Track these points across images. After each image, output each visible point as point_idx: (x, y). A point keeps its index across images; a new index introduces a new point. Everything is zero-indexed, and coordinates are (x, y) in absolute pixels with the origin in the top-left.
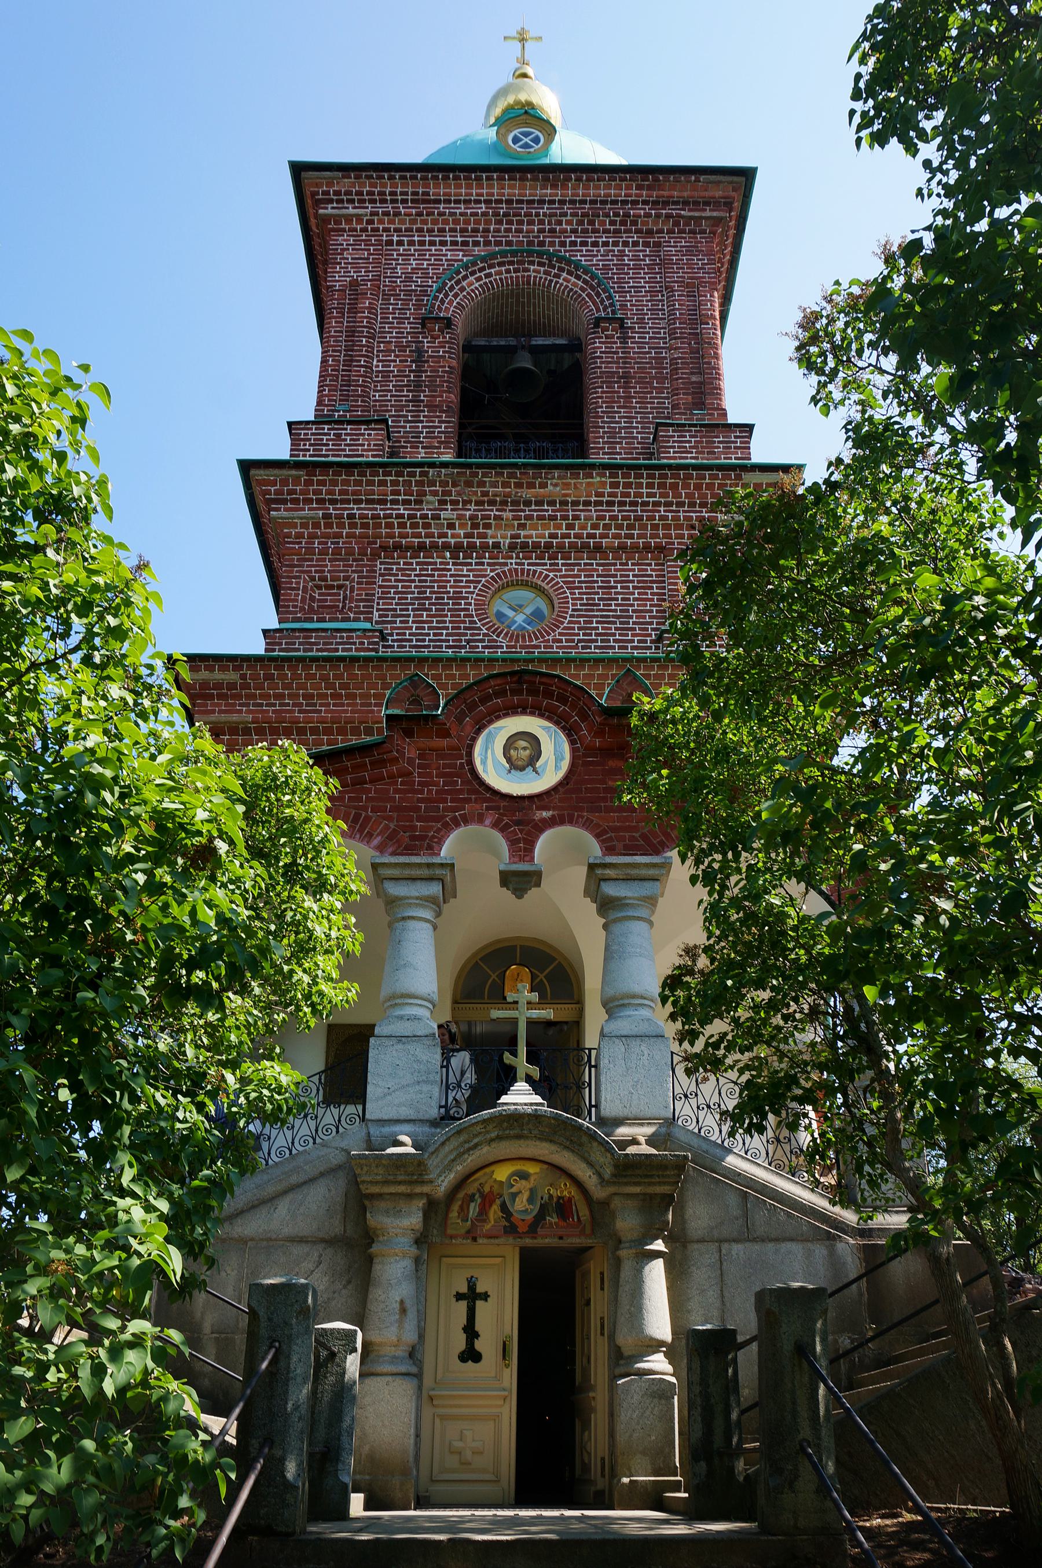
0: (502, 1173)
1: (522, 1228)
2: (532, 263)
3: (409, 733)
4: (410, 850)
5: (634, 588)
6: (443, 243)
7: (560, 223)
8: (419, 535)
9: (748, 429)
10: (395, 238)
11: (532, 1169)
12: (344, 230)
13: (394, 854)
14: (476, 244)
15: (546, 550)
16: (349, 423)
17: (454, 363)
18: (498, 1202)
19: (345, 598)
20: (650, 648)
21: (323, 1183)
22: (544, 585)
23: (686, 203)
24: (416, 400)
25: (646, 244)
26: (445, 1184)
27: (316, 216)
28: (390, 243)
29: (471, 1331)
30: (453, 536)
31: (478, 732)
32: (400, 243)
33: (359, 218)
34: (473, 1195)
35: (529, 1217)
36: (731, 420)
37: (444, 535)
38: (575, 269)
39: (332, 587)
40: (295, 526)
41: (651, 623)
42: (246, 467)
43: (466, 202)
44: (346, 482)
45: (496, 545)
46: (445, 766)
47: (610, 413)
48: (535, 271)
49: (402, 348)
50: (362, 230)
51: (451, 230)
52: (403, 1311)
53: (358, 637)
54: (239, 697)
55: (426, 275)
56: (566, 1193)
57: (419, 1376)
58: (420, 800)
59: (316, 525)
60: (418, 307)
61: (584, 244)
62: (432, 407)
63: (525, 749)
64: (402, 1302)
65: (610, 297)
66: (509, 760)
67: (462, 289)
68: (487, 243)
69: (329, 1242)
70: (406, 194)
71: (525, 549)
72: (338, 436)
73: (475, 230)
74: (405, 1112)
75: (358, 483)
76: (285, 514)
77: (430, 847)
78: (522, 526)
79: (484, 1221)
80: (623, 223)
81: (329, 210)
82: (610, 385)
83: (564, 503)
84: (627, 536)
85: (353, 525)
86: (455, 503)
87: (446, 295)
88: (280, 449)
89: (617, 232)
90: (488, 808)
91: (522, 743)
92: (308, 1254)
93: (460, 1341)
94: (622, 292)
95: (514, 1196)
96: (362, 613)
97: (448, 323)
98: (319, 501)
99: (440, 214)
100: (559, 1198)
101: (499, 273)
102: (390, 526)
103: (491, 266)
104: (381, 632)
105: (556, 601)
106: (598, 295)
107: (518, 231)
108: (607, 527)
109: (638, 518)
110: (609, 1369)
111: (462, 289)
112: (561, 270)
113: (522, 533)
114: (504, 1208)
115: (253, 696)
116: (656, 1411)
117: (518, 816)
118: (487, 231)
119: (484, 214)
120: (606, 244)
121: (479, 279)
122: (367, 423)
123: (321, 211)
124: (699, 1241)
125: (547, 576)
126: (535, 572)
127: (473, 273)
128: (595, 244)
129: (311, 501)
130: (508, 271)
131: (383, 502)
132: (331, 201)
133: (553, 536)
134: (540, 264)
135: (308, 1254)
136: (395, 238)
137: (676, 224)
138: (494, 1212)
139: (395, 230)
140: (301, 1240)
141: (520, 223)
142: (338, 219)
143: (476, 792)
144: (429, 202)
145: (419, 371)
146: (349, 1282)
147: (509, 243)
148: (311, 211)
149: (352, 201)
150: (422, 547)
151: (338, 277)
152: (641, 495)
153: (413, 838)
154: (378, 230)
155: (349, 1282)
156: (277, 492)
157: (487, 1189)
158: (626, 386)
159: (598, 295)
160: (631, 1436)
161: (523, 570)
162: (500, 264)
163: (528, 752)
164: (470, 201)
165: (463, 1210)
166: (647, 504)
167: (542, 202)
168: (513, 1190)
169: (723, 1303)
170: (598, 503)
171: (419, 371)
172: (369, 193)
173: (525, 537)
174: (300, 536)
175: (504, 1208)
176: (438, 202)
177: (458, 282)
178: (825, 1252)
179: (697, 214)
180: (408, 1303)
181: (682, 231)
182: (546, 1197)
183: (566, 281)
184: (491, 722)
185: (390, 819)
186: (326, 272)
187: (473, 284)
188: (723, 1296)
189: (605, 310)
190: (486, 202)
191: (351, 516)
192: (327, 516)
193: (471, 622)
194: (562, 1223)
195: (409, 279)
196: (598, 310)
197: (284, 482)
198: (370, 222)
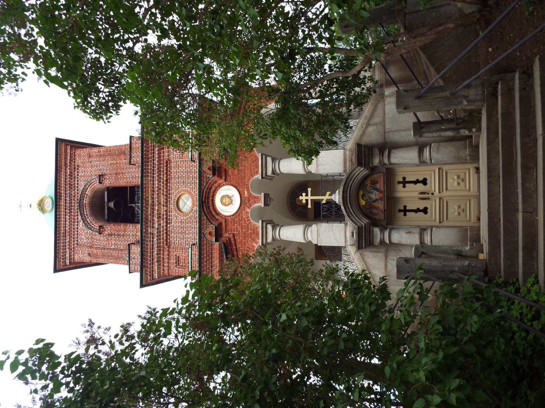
0: (363, 203)
1: (381, 195)
2: (83, 202)
3: (221, 235)
4: (257, 234)
5: (178, 169)
6: (77, 228)
7: (72, 194)
9: (131, 137)
10: (76, 242)
11: (361, 193)
12: (74, 257)
13: (259, 239)
14: (78, 218)
15: (167, 197)
16: (129, 255)
17: (112, 225)
18: (372, 203)
19: (182, 256)
20: (197, 164)
21: (366, 259)
22: (178, 197)
24: (123, 235)
25: (78, 169)
26: (366, 220)
27: (69, 265)
28: (77, 244)
29: (417, 211)
30: (163, 224)
31: (220, 214)
32: (77, 241)
33: (70, 253)
34: (370, 211)
35: (377, 193)
36: (128, 143)
37: (163, 226)
38: (85, 190)
39: (178, 260)
41: (189, 164)
42: (142, 285)
43: (65, 222)
45: (166, 211)
46: (231, 224)
47: (127, 178)
48: (86, 201)
49: (108, 240)
50: (74, 252)
52: (410, 232)
53: (194, 252)
55: (87, 233)
56: (369, 182)
57: (432, 227)
58: (242, 231)
59: (160, 265)
60: (96, 235)
61: (78, 187)
62: (125, 231)
63: (226, 200)
64: (406, 233)
65: (93, 179)
66: (229, 204)
67: (91, 222)
68: (77, 215)
69: (386, 257)
70: (63, 239)
72: (133, 258)
74: (343, 234)
77: (257, 228)
78: (160, 203)
79: (379, 208)
80: (72, 176)
81: (68, 262)
82: (118, 178)
84: (163, 172)
85: (160, 254)
87: (93, 227)
88: (137, 276)
90: (244, 210)
91: (224, 200)
92: (391, 264)
93: (422, 214)
94: (92, 176)
95: (370, 198)
96: (186, 251)
97: (101, 227)
98: (153, 264)
99: (69, 229)
100: (371, 184)
102: (160, 243)
103: (84, 214)
104: (192, 245)
105: (183, 193)
106: (92, 183)
108: (160, 178)
109: (158, 169)
110: (429, 166)
111: (91, 222)
113: (162, 203)
114: (375, 201)
116: (444, 149)
117: (247, 201)
119: (69, 216)
120: (78, 181)
121: (88, 218)
122: (129, 250)
123: (68, 264)
124: (385, 139)
125: (175, 196)
126: (174, 199)
127: (86, 219)
128: (78, 184)
130: (86, 209)
131: (153, 244)
132: (65, 261)
135: (391, 264)
136: (76, 242)
138: (376, 204)
139: (74, 242)
140: (386, 266)
141: (72, 206)
142: (70, 259)
143: (239, 214)
144: (65, 232)
145: (114, 235)
146: (400, 250)
147: (77, 209)
148: (68, 267)
149: (65, 255)
150: (167, 233)
151: (87, 259)
153: (254, 233)
154: (74, 247)
155: (400, 250)
157: (368, 207)
158: (119, 174)
159: (92, 183)
160: (453, 157)
161: (173, 203)
162: (84, 212)
163: (227, 199)
164: (65, 221)
165: (375, 214)
166: (153, 166)
168: (368, 199)
169: (406, 130)
171: (114, 235)
173: (163, 202)
175: (375, 201)
176: (65, 230)
177: (89, 224)
178: (388, 98)
179: (69, 155)
180: (407, 231)
181: (74, 158)
182: (371, 188)
183: (89, 192)
184: (217, 210)
185: (248, 240)
186: (86, 263)
187: (89, 219)
188: (404, 130)
189: (96, 180)
190: (65, 216)
193: (189, 218)
194: (379, 183)
196: (97, 183)
198: (71, 250)
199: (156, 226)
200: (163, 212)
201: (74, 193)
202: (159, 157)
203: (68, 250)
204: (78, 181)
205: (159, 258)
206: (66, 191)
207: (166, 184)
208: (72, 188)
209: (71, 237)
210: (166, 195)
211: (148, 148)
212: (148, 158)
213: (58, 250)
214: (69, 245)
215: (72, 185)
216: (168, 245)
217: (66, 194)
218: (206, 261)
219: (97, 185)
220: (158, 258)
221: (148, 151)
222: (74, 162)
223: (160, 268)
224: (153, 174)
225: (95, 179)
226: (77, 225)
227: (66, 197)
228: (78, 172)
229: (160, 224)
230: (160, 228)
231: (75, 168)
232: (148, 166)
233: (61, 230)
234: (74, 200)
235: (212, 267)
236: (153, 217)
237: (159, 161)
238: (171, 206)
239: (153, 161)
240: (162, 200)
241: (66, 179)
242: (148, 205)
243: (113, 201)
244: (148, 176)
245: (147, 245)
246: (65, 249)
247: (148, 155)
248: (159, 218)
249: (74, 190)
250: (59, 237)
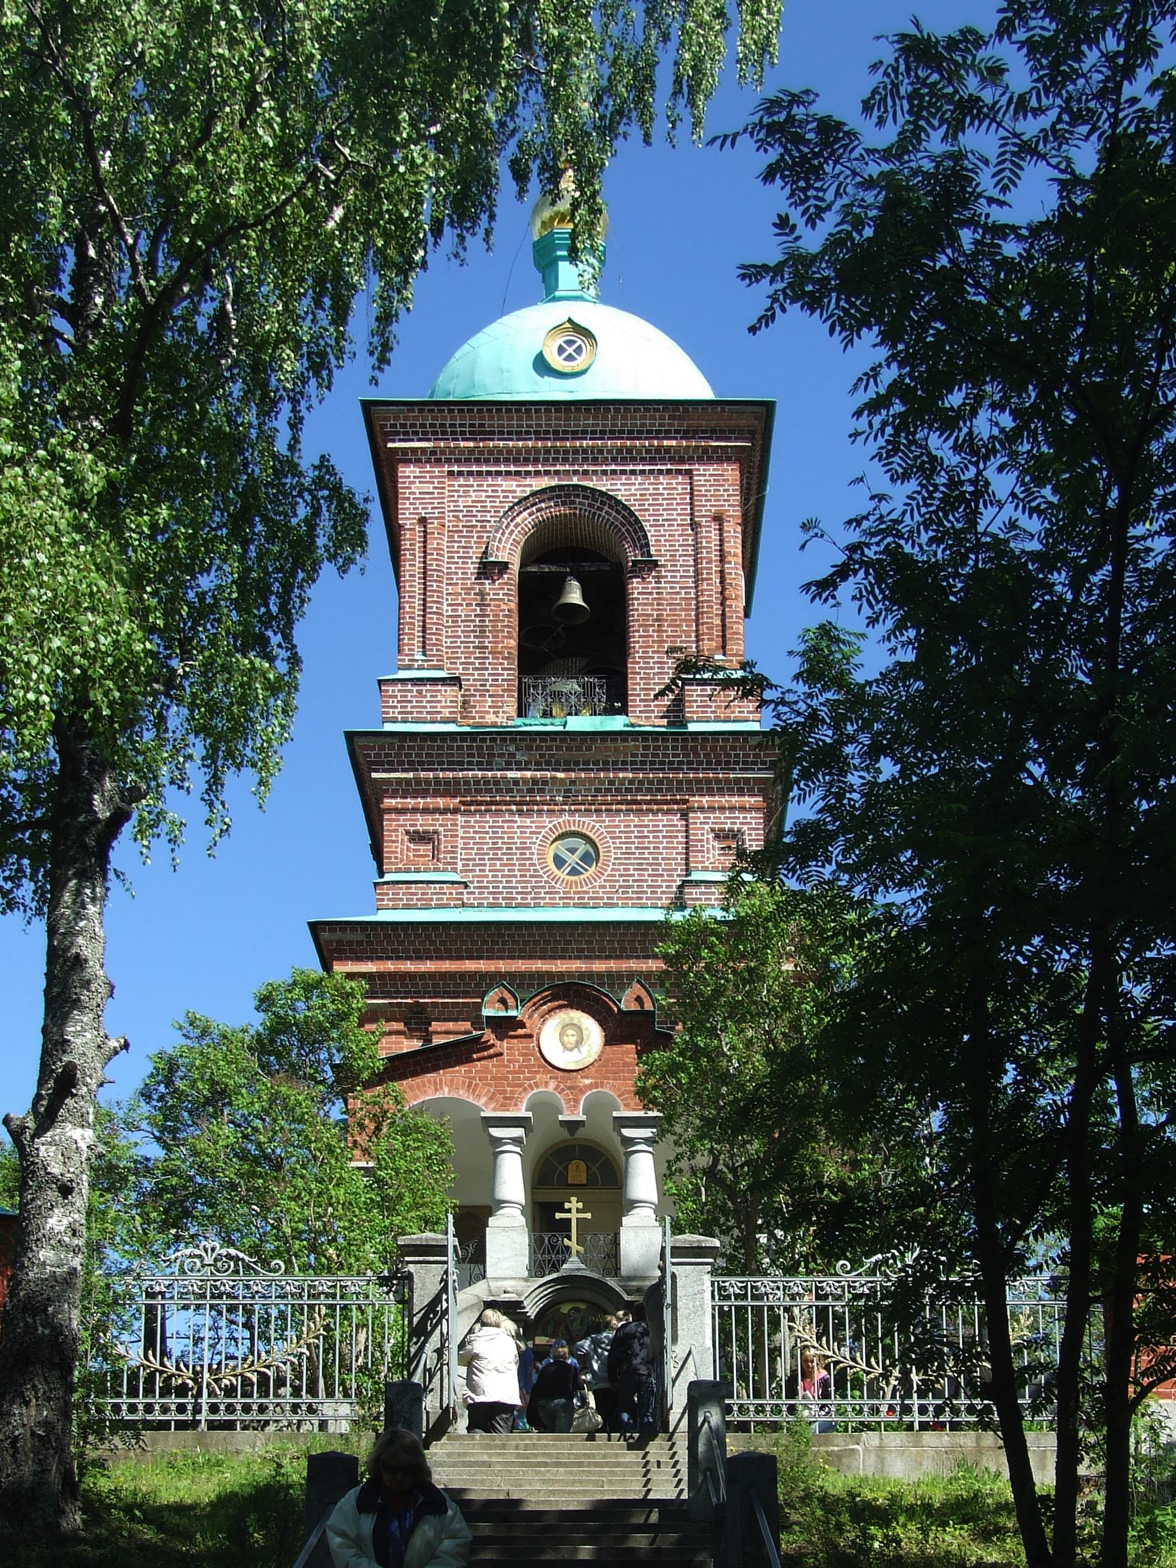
2: (577, 496)
42: (350, 736)
67: (517, 526)
75: (441, 748)
112: (603, 503)
129: (402, 763)
132: (398, 433)
172: (432, 425)
195: (470, 514)
197: (382, 748)
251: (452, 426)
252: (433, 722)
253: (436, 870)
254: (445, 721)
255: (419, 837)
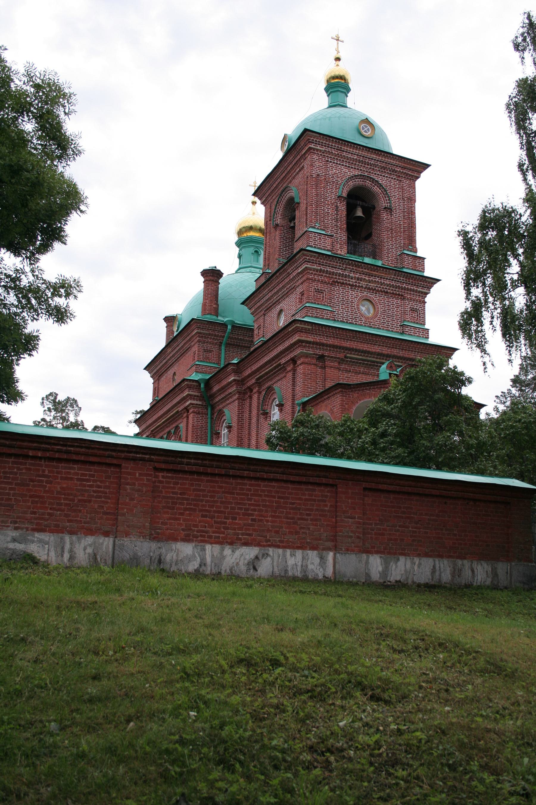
6: (343, 165)
7: (376, 167)
8: (343, 280)
19: (323, 296)
23: (410, 170)
25: (398, 180)
32: (331, 162)
33: (320, 151)
38: (380, 186)
39: (319, 292)
40: (311, 270)
44: (327, 260)
45: (362, 287)
48: (368, 183)
50: (321, 155)
51: (346, 161)
54: (310, 333)
59: (317, 271)
61: (381, 175)
71: (369, 289)
73: (352, 163)
75: (331, 261)
76: (310, 266)
78: (370, 282)
80: (393, 172)
83: (381, 278)
85: (327, 273)
86: (354, 272)
89: (391, 174)
99: (344, 156)
101: (358, 181)
107: (364, 167)
108: (390, 287)
112: (375, 185)
115: (313, 334)
118: (355, 164)
119: (356, 159)
120: (387, 177)
128: (384, 176)
131: (336, 268)
132: (313, 143)
133: (377, 287)
134: (370, 181)
137: (407, 175)
139: (330, 157)
141: (365, 164)
142: (314, 149)
147: (361, 170)
150: (343, 283)
152: (400, 279)
156: (309, 259)
162: (359, 179)
167: (372, 159)
170: (390, 279)
174: (312, 273)
176: (344, 151)
179: (413, 174)
181: (408, 178)
183: (376, 189)
187: (351, 184)
190: (357, 155)
191: (327, 271)
192: (321, 269)
195: (333, 177)
198: (323, 153)
199: (352, 275)
200: (363, 284)
201: (376, 170)
202: (408, 289)
203: (324, 149)
204: (387, 177)
205: (324, 271)
206: (380, 161)
207: (384, 291)
208: (381, 168)
209: (336, 156)
210: (375, 289)
211: (418, 281)
212: (409, 279)
213: (326, 139)
214: (329, 151)
215: (384, 169)
216: (334, 283)
217: (378, 161)
218: (333, 333)
219: (383, 203)
220: (324, 271)
221: (415, 280)
222: (405, 178)
223: (314, 271)
224: (395, 281)
225: (389, 203)
226: (346, 166)
227: (375, 160)
228: (395, 179)
229: (352, 279)
230: (349, 278)
231: (399, 176)
232: (403, 277)
233: (344, 146)
234: (370, 168)
235: (327, 336)
236: (360, 273)
237: (405, 289)
238: (365, 294)
239: (406, 283)
240: (372, 285)
241: (392, 164)
242: (371, 270)
243: (363, 214)
244: (395, 275)
245: (337, 262)
246: (325, 146)
247: (412, 279)
248: (358, 279)
249: (379, 171)
250: (339, 142)
251: (332, 145)
252: (324, 250)
253: (325, 305)
254: (328, 250)
255: (318, 291)
